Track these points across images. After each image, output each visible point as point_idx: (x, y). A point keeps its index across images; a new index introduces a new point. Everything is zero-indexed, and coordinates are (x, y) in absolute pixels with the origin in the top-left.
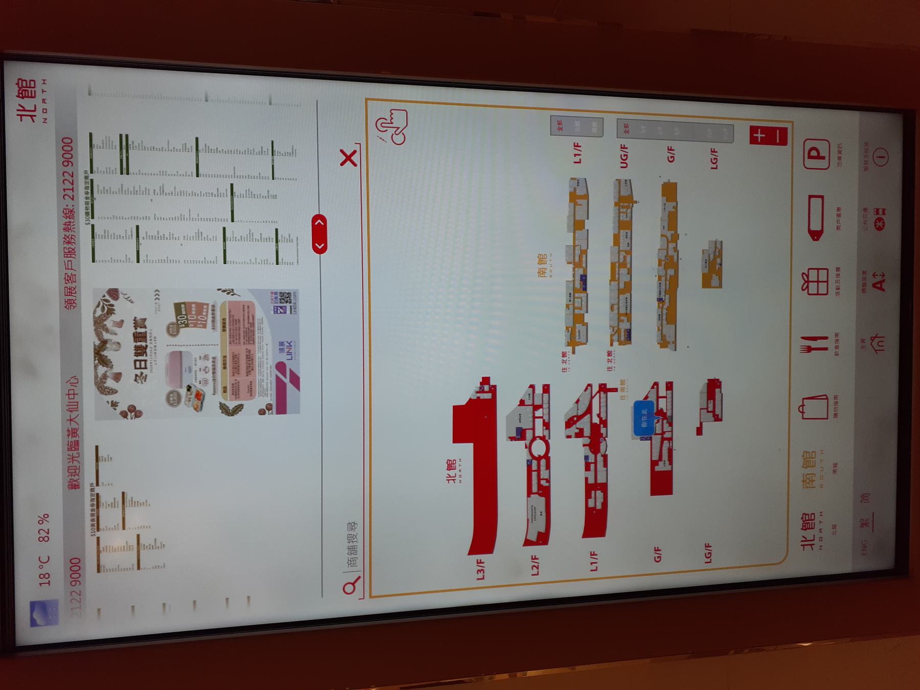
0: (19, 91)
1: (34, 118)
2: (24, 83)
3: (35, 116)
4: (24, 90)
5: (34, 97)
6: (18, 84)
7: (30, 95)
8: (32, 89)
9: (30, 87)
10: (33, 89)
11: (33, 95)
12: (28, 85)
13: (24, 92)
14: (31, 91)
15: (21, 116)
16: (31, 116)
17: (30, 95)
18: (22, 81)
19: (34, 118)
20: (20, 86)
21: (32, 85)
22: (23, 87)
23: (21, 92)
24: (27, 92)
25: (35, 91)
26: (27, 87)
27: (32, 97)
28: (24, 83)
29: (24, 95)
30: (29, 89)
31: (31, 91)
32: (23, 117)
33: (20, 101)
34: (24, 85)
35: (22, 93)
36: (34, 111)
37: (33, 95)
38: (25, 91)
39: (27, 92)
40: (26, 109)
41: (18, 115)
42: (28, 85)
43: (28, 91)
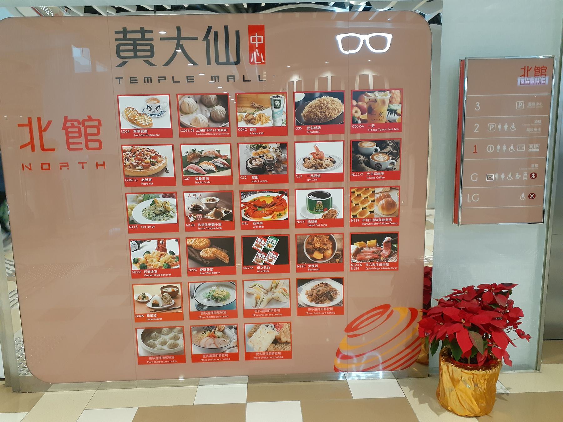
1: (29, 147)
2: (94, 131)
3: (33, 150)
6: (90, 119)
8: (84, 143)
9: (87, 141)
10: (83, 146)
11: (72, 146)
12: (90, 138)
13: (76, 130)
14: (81, 143)
15: (30, 125)
17: (71, 140)
18: (98, 128)
20: (87, 124)
21: (91, 145)
22: (86, 128)
23: (76, 124)
24: (77, 135)
25: (81, 149)
26: (86, 135)
27: (68, 144)
28: (94, 131)
29: (70, 130)
30: (82, 139)
31: (81, 143)
34: (90, 131)
35: (73, 126)
39: (77, 135)
41: (30, 119)
43: (80, 136)
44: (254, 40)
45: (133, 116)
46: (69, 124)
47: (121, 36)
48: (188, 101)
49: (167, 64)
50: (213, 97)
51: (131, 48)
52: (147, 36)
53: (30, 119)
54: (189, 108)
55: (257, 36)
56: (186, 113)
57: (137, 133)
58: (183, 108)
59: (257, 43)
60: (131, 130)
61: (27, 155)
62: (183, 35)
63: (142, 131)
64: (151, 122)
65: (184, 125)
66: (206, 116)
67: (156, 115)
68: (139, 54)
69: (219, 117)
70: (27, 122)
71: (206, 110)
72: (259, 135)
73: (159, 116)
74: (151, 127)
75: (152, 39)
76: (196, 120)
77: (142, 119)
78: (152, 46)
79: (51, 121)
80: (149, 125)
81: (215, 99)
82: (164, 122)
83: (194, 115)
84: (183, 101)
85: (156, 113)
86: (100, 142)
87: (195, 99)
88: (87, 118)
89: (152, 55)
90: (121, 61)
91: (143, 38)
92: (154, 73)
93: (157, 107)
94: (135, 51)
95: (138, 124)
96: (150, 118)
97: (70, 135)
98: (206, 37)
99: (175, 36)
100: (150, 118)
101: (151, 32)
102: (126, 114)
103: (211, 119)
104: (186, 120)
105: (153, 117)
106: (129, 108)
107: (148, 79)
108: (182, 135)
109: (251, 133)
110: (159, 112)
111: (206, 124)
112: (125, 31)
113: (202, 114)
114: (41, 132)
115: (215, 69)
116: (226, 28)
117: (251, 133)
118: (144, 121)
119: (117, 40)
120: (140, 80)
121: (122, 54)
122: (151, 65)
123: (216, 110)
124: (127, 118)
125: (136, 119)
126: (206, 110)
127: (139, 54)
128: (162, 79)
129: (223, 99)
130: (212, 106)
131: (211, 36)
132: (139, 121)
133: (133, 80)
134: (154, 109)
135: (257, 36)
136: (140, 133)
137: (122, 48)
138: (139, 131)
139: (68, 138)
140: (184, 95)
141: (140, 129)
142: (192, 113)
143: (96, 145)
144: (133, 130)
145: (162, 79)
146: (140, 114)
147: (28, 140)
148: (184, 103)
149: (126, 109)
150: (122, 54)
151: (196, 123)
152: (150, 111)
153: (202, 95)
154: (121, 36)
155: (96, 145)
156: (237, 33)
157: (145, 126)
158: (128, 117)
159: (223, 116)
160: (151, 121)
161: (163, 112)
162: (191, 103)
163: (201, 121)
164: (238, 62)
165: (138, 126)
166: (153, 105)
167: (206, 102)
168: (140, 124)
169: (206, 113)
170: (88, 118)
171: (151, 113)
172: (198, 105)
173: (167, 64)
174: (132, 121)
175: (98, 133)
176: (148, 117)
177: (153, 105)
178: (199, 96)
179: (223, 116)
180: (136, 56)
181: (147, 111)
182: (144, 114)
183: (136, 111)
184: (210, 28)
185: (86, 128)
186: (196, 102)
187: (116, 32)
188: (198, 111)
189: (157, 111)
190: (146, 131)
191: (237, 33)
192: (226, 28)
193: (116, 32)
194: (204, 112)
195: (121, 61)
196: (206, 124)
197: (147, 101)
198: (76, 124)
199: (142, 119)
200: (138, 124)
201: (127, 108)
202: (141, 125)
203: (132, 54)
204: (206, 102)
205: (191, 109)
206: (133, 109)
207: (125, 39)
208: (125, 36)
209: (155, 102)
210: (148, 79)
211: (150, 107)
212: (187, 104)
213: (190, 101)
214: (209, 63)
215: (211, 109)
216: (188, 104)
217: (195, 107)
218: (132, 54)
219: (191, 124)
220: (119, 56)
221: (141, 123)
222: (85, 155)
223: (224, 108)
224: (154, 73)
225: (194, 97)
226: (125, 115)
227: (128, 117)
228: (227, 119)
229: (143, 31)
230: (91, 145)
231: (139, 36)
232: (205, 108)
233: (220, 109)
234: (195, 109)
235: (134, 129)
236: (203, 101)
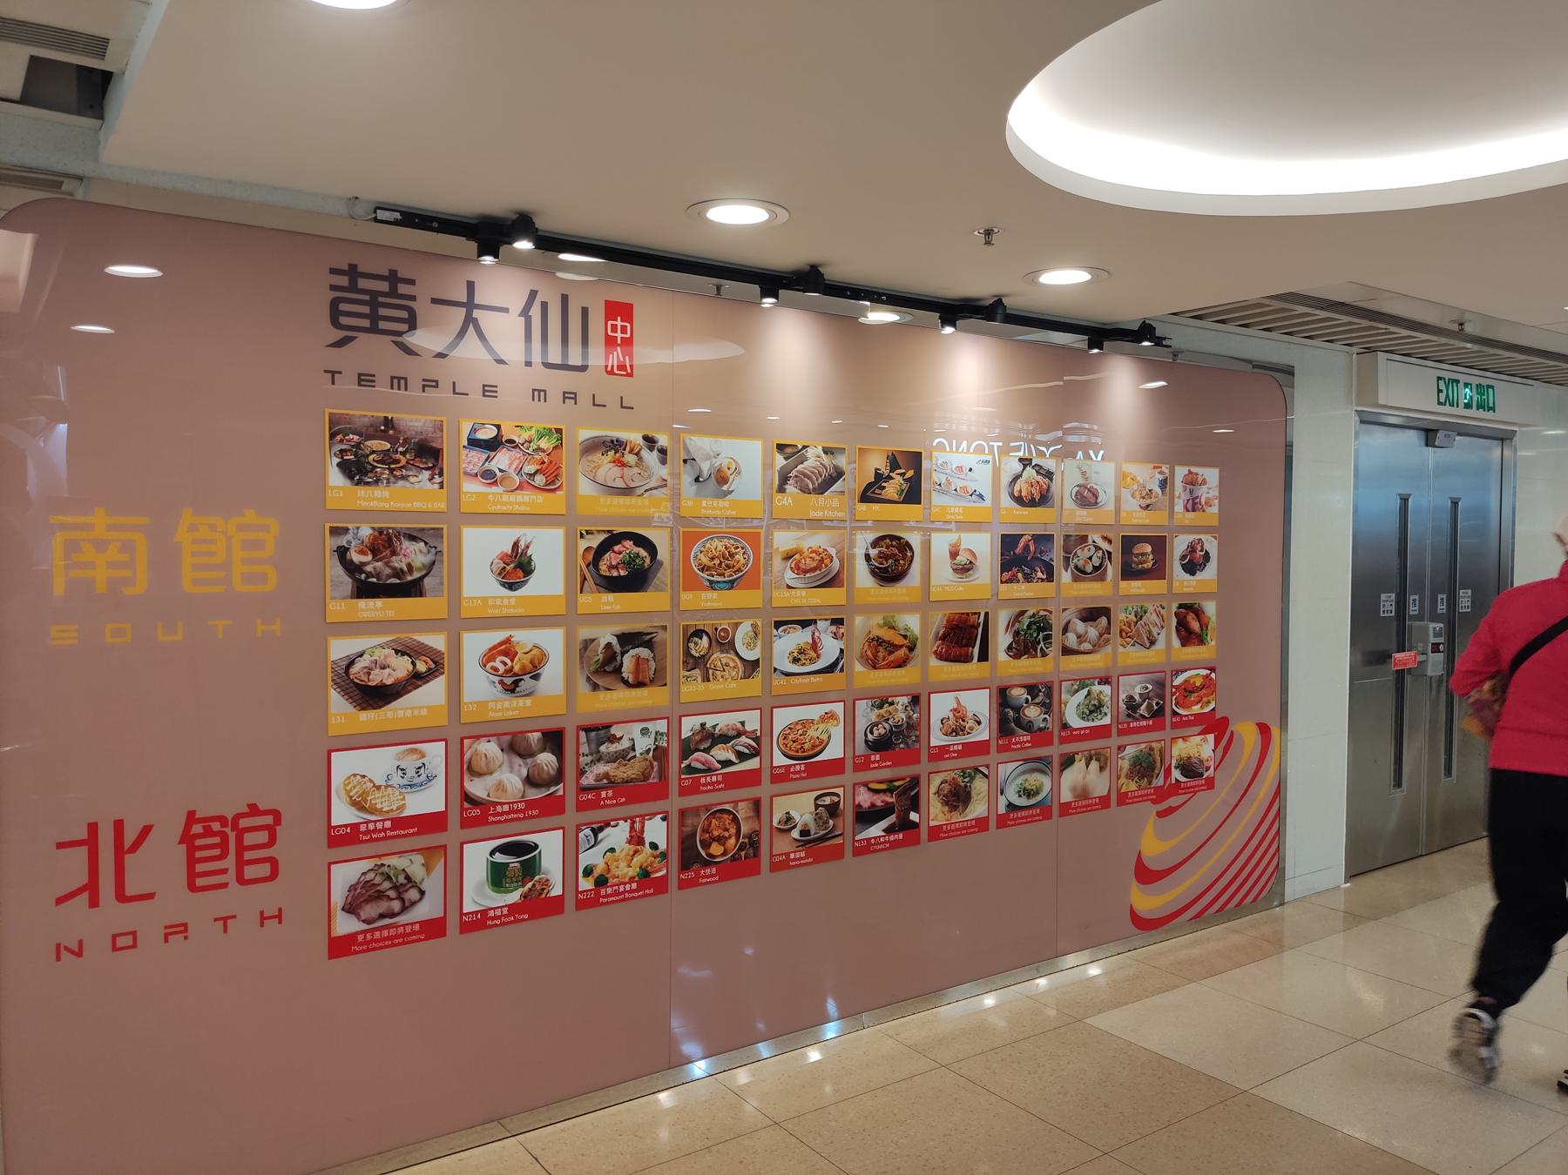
0: (222, 820)
1: (85, 897)
2: (263, 837)
3: (94, 902)
4: (224, 836)
5: (193, 887)
6: (254, 810)
7: (200, 868)
9: (241, 863)
10: (230, 877)
11: (200, 882)
12: (248, 855)
14: (224, 871)
15: (91, 840)
16: (91, 889)
17: (200, 868)
18: (272, 830)
19: (85, 897)
20: (244, 823)
22: (240, 833)
25: (224, 886)
26: (241, 848)
27: (192, 876)
28: (263, 837)
30: (230, 862)
31: (224, 871)
32: (84, 850)
33: (169, 830)
34: (250, 839)
35: (208, 832)
36: (121, 896)
37: (200, 882)
38: (224, 846)
39: (217, 852)
40: (129, 859)
41: (93, 828)
42: (248, 855)
45: (363, 792)
46: (197, 829)
48: (486, 750)
50: (535, 737)
53: (93, 828)
54: (487, 764)
56: (480, 775)
57: (368, 832)
58: (474, 764)
60: (355, 826)
61: (78, 920)
63: (379, 826)
64: (403, 802)
65: (475, 801)
66: (519, 776)
67: (414, 785)
69: (545, 776)
70: (83, 834)
71: (520, 765)
72: (617, 804)
73: (423, 787)
74: (402, 812)
76: (500, 786)
77: (382, 797)
79: (152, 826)
80: (398, 808)
81: (539, 740)
82: (431, 800)
83: (496, 776)
84: (476, 751)
85: (417, 780)
86: (274, 863)
87: (500, 745)
88: (246, 810)
93: (419, 768)
95: (372, 811)
96: (401, 793)
97: (199, 854)
100: (401, 793)
102: (346, 790)
103: (530, 781)
104: (477, 788)
105: (409, 790)
106: (355, 775)
108: (466, 823)
109: (602, 802)
110: (423, 777)
111: (520, 790)
113: (511, 772)
114: (120, 853)
117: (602, 802)
118: (386, 803)
123: (539, 762)
124: (348, 799)
125: (369, 798)
126: (520, 765)
129: (554, 740)
130: (532, 755)
132: (376, 804)
134: (411, 772)
136: (375, 831)
138: (371, 826)
139: (192, 861)
140: (478, 737)
141: (375, 822)
142: (491, 773)
143: (264, 870)
144: (357, 825)
146: (378, 788)
147: (82, 878)
148: (477, 755)
149: (346, 780)
151: (500, 791)
152: (403, 778)
153: (514, 734)
155: (264, 870)
157: (388, 812)
158: (351, 797)
159: (552, 772)
160: (404, 799)
161: (429, 779)
162: (490, 753)
163: (508, 789)
165: (372, 813)
166: (410, 763)
167: (522, 749)
168: (376, 809)
169: (519, 771)
170: (248, 811)
171: (405, 782)
172: (505, 756)
174: (358, 805)
175: (272, 841)
176: (397, 793)
177: (410, 763)
178: (508, 738)
179: (552, 772)
181: (397, 780)
182: (390, 786)
183: (370, 780)
185: (240, 833)
186: (502, 750)
188: (505, 767)
189: (419, 776)
190: (388, 824)
194: (516, 768)
196: (520, 790)
197: (400, 757)
198: (216, 826)
199: (382, 797)
200: (372, 811)
201: (349, 777)
202: (380, 811)
204: (522, 749)
205: (492, 766)
206: (364, 776)
209: (415, 756)
211: (402, 770)
212: (483, 756)
213: (490, 748)
215: (529, 761)
216: (486, 755)
217: (499, 761)
219: (488, 796)
221: (379, 806)
222: (235, 898)
223: (554, 757)
225: (498, 739)
226: (343, 792)
227: (351, 797)
228: (559, 777)
230: (250, 872)
232: (518, 760)
233: (547, 759)
234: (498, 764)
235: (361, 823)
236: (515, 747)
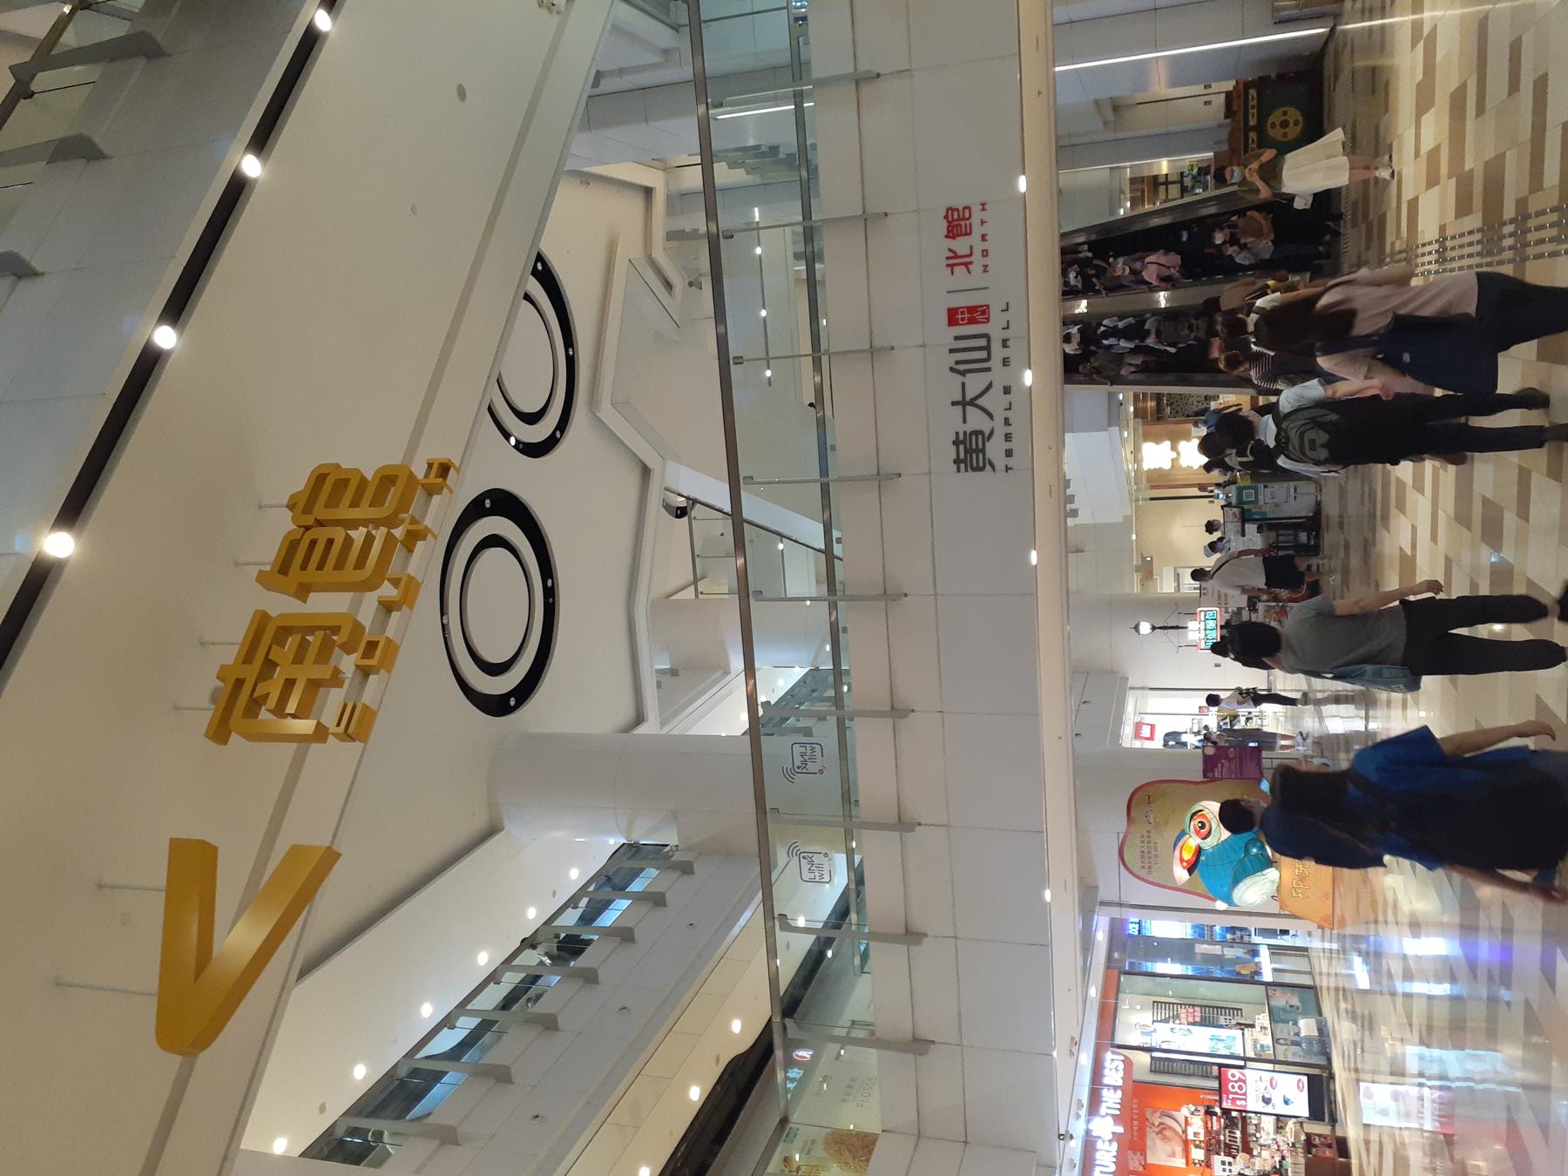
44: (963, 319)
47: (962, 466)
49: (991, 416)
51: (974, 455)
52: (961, 438)
55: (959, 316)
59: (966, 316)
62: (959, 398)
68: (980, 446)
75: (965, 433)
78: (973, 433)
89: (982, 433)
90: (988, 467)
91: (964, 442)
92: (1000, 431)
94: (977, 451)
98: (963, 373)
99: (959, 408)
101: (957, 433)
107: (1008, 437)
112: (957, 462)
115: (996, 362)
116: (951, 351)
119: (966, 471)
120: (1008, 445)
121: (981, 465)
122: (991, 433)
127: (980, 446)
128: (1007, 422)
131: (962, 367)
133: (1009, 453)
135: (959, 316)
137: (975, 465)
145: (1007, 422)
150: (981, 465)
154: (962, 466)
156: (956, 338)
164: (987, 336)
173: (991, 416)
180: (983, 450)
184: (952, 369)
187: (959, 471)
191: (956, 338)
192: (951, 351)
193: (959, 471)
195: (988, 467)
203: (981, 455)
207: (964, 461)
208: (962, 461)
210: (1008, 437)
214: (988, 369)
218: (981, 455)
220: (982, 469)
224: (1000, 431)
229: (956, 443)
231: (962, 448)
